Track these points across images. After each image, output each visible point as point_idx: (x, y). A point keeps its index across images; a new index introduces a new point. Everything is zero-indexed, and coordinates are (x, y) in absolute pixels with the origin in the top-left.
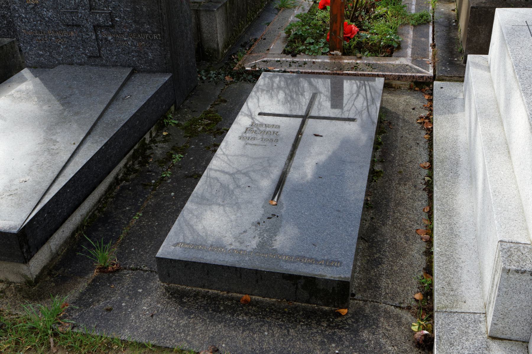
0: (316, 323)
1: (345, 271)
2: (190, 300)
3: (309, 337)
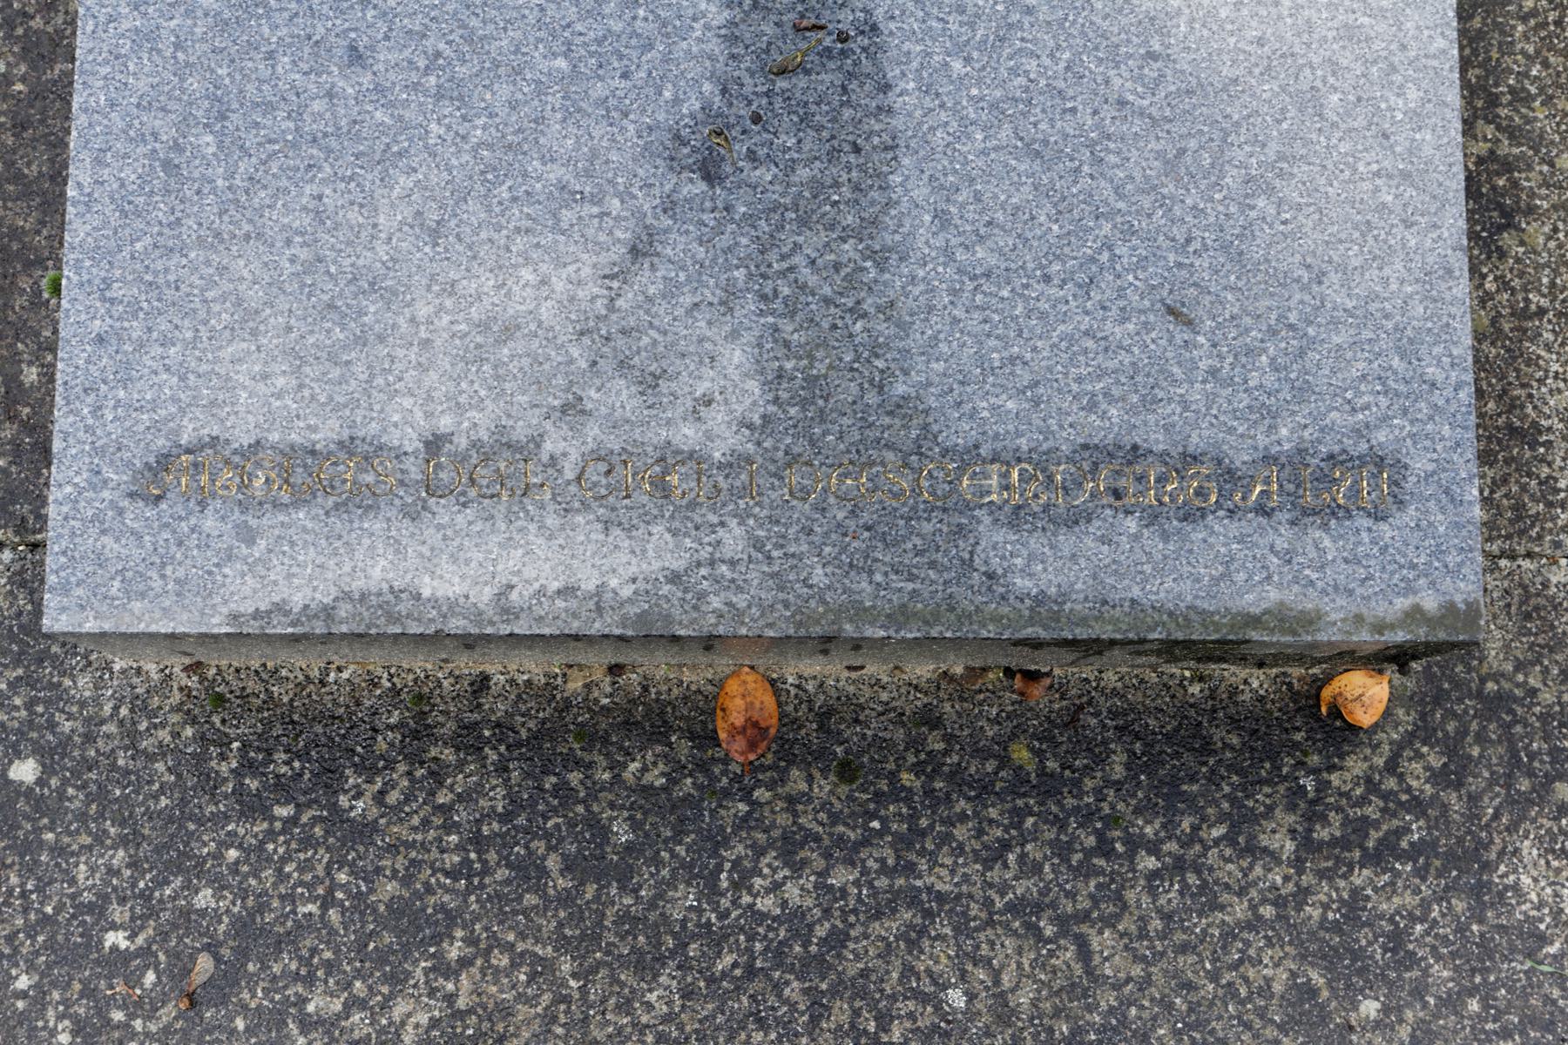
0: (1230, 839)
1: (1438, 552)
2: (393, 797)
3: (1214, 977)
